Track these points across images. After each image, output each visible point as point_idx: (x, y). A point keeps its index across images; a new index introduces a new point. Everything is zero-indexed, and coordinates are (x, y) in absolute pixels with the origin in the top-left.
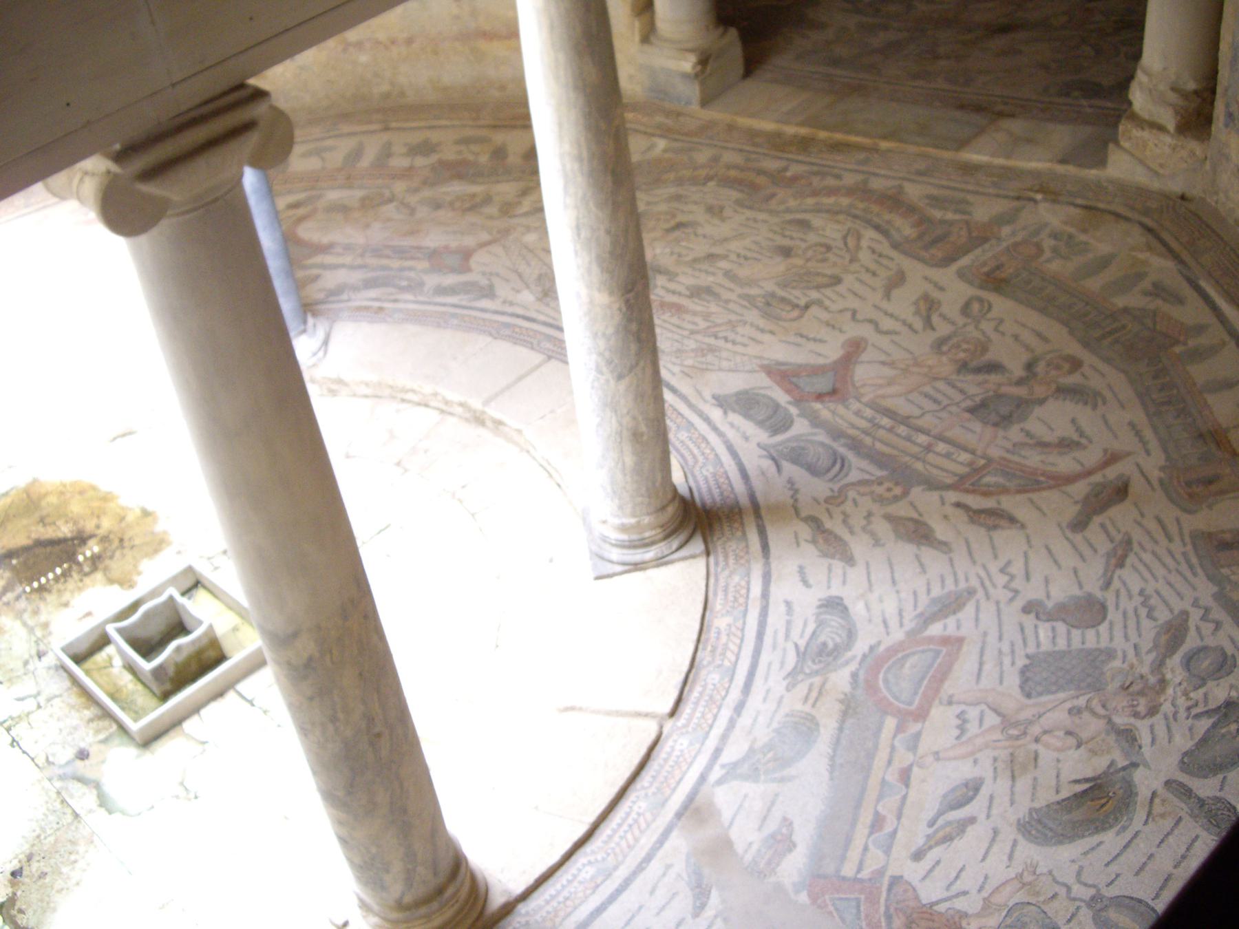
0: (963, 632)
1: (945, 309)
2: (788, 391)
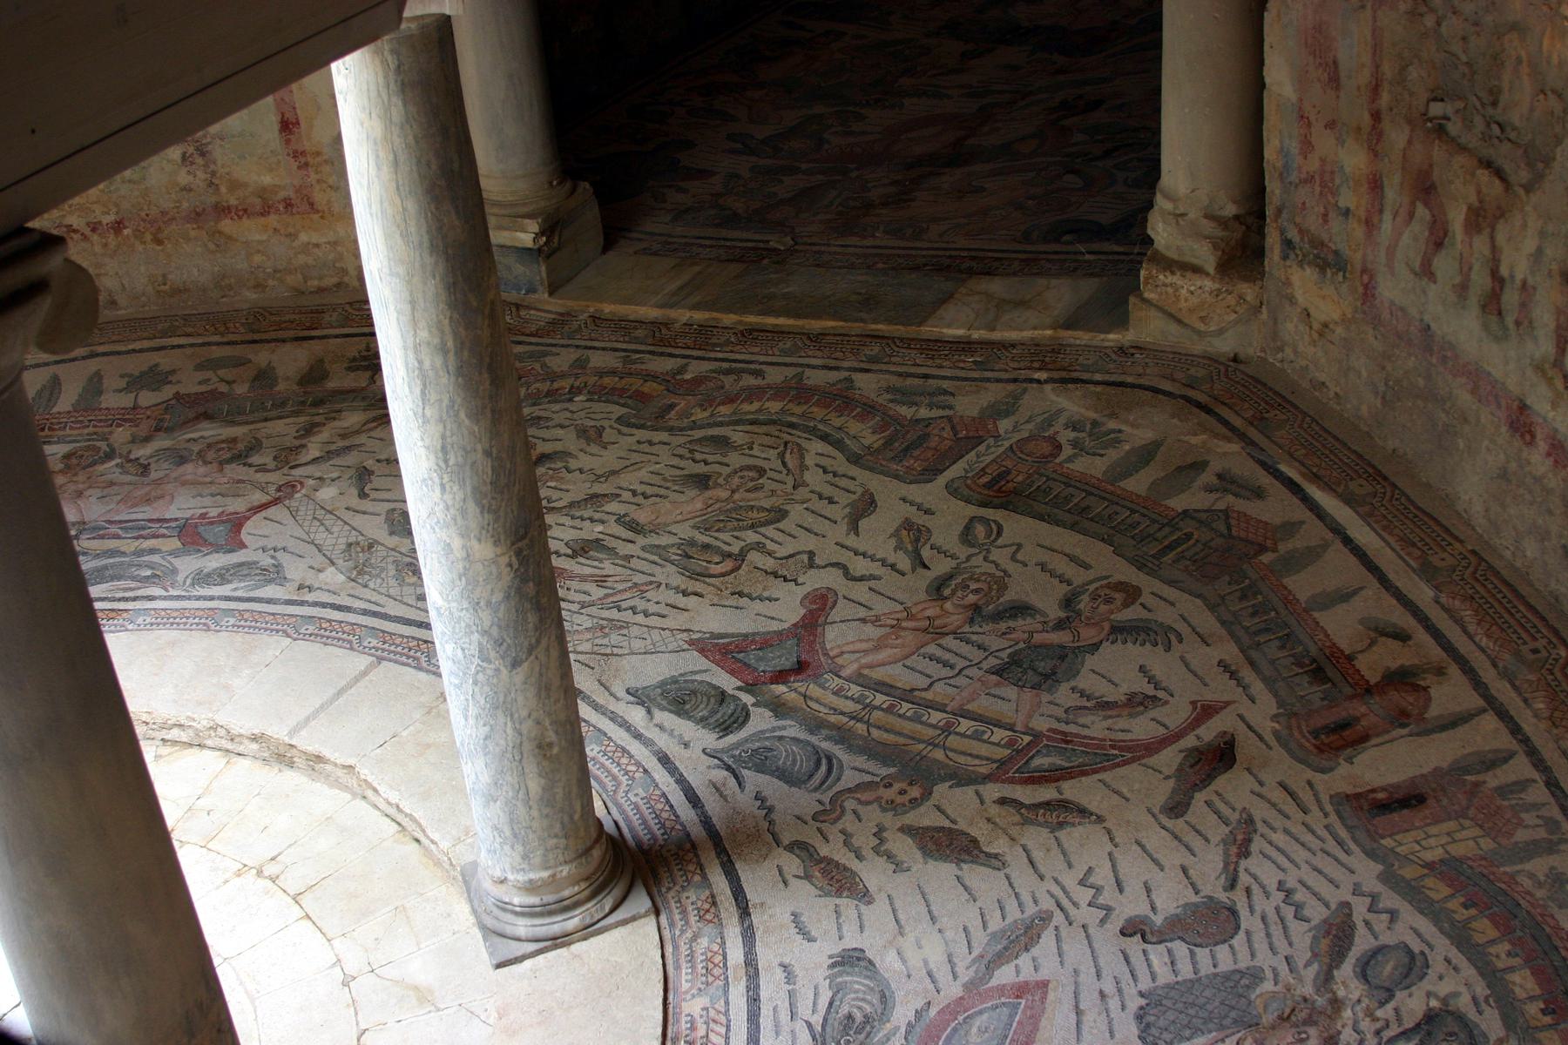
0: (1044, 974)
1: (937, 538)
2: (732, 672)
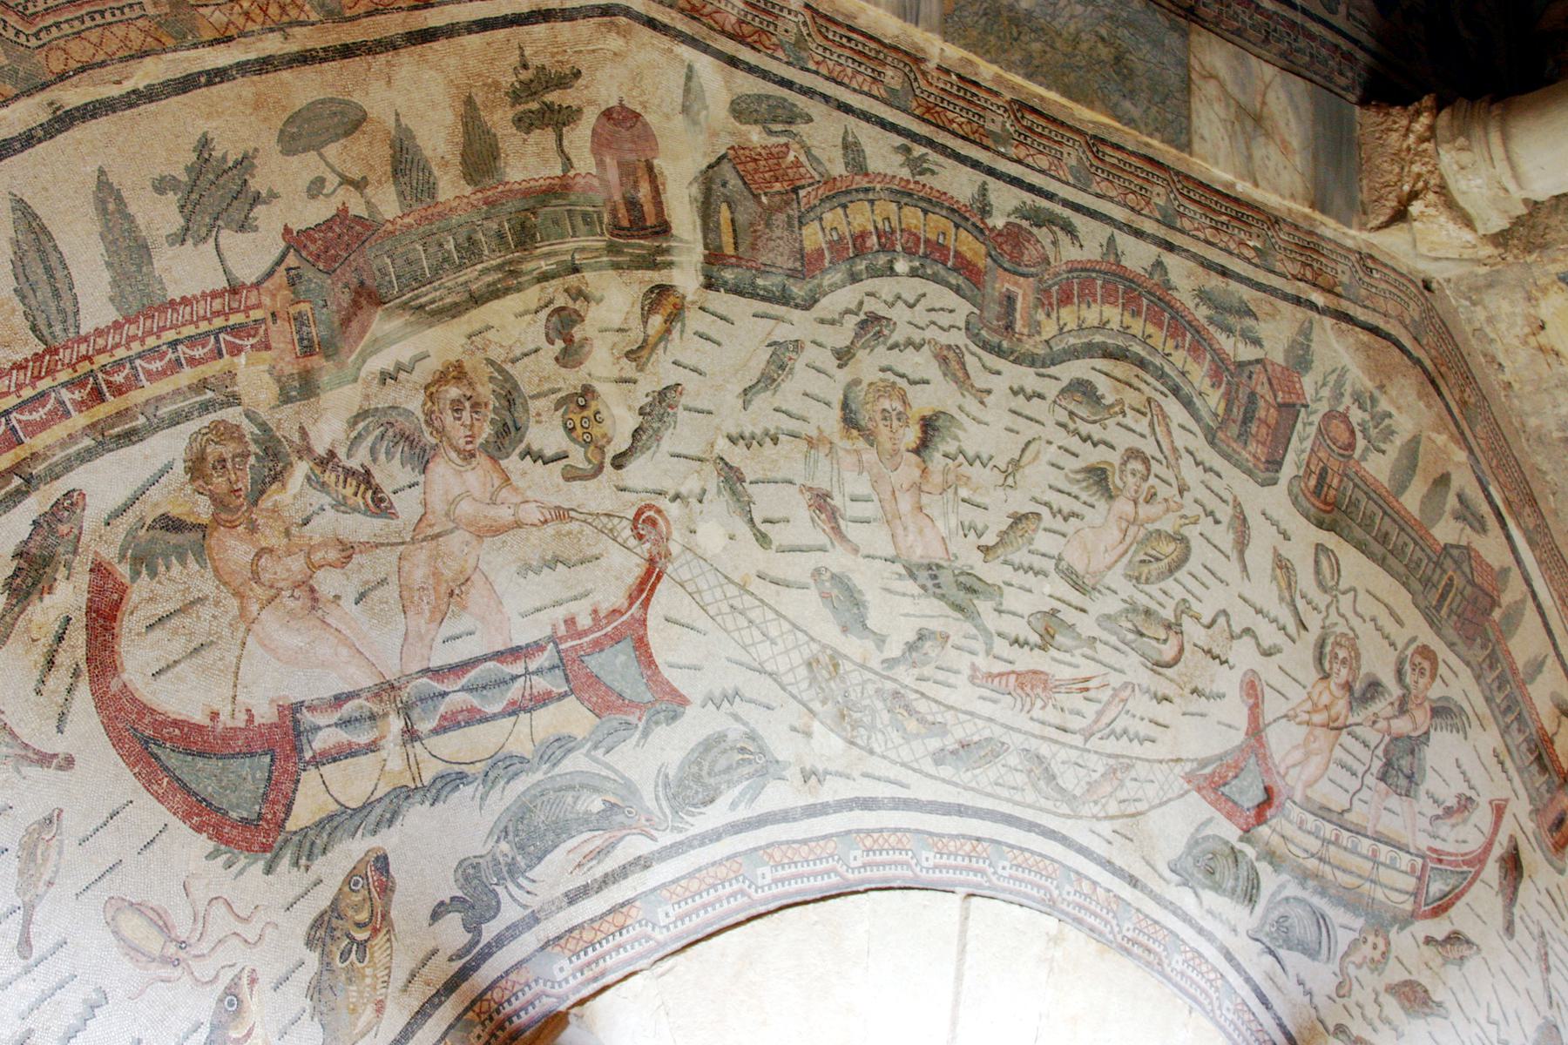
2: (1229, 816)
